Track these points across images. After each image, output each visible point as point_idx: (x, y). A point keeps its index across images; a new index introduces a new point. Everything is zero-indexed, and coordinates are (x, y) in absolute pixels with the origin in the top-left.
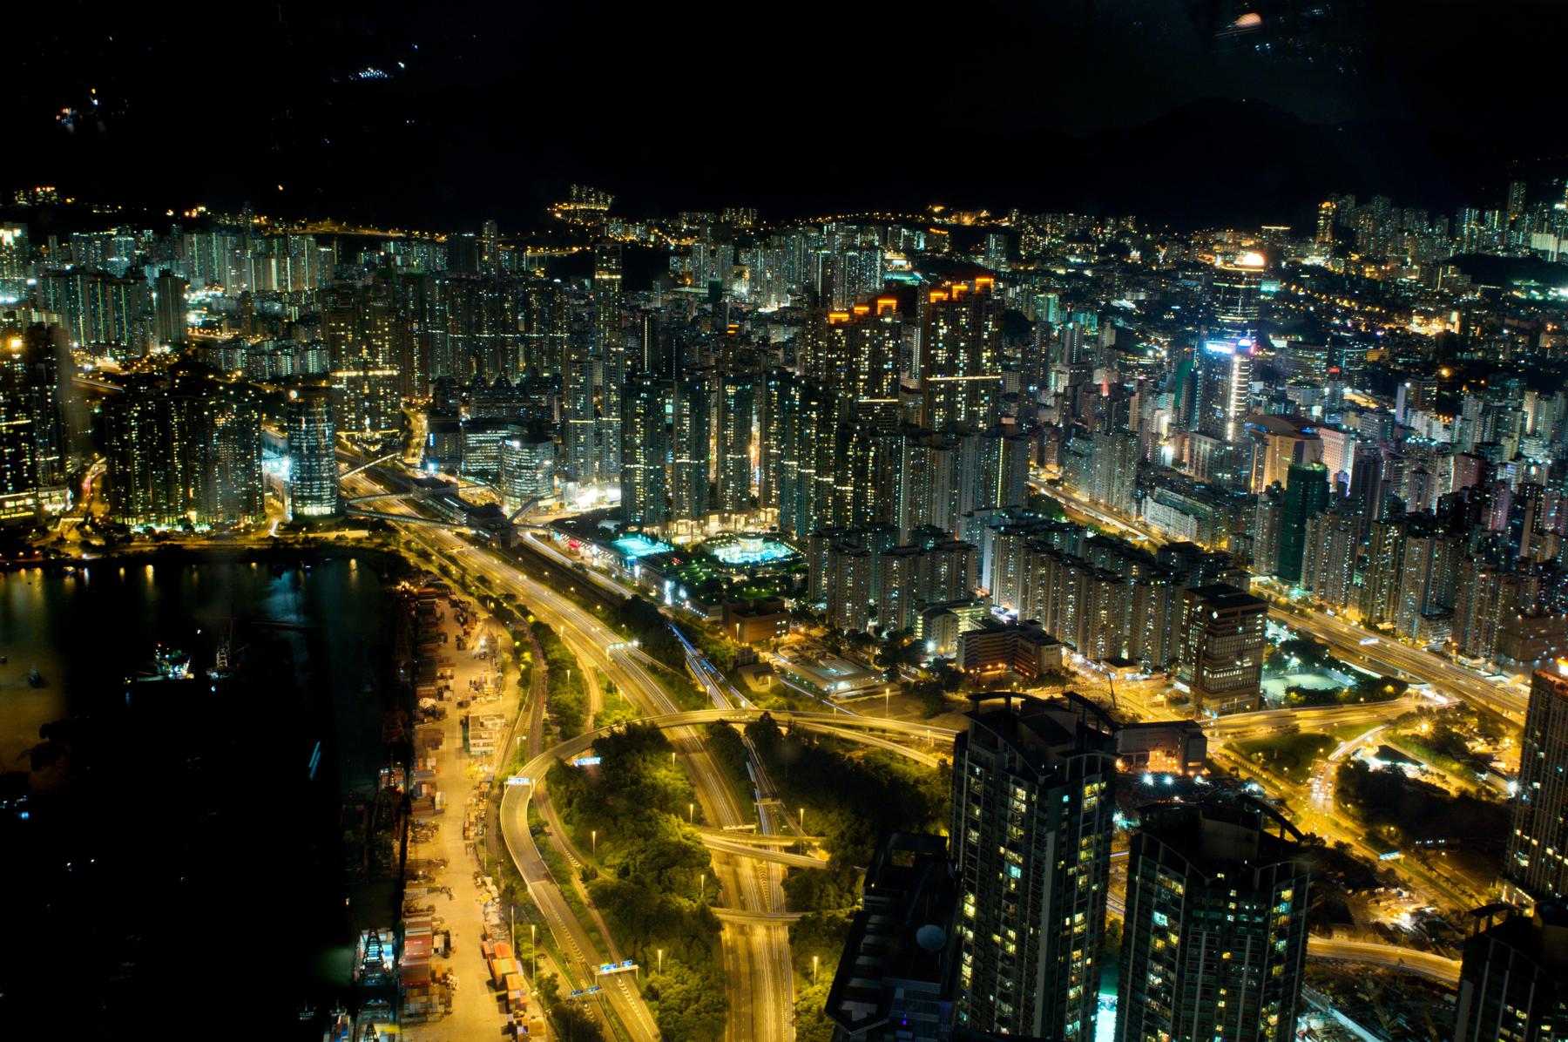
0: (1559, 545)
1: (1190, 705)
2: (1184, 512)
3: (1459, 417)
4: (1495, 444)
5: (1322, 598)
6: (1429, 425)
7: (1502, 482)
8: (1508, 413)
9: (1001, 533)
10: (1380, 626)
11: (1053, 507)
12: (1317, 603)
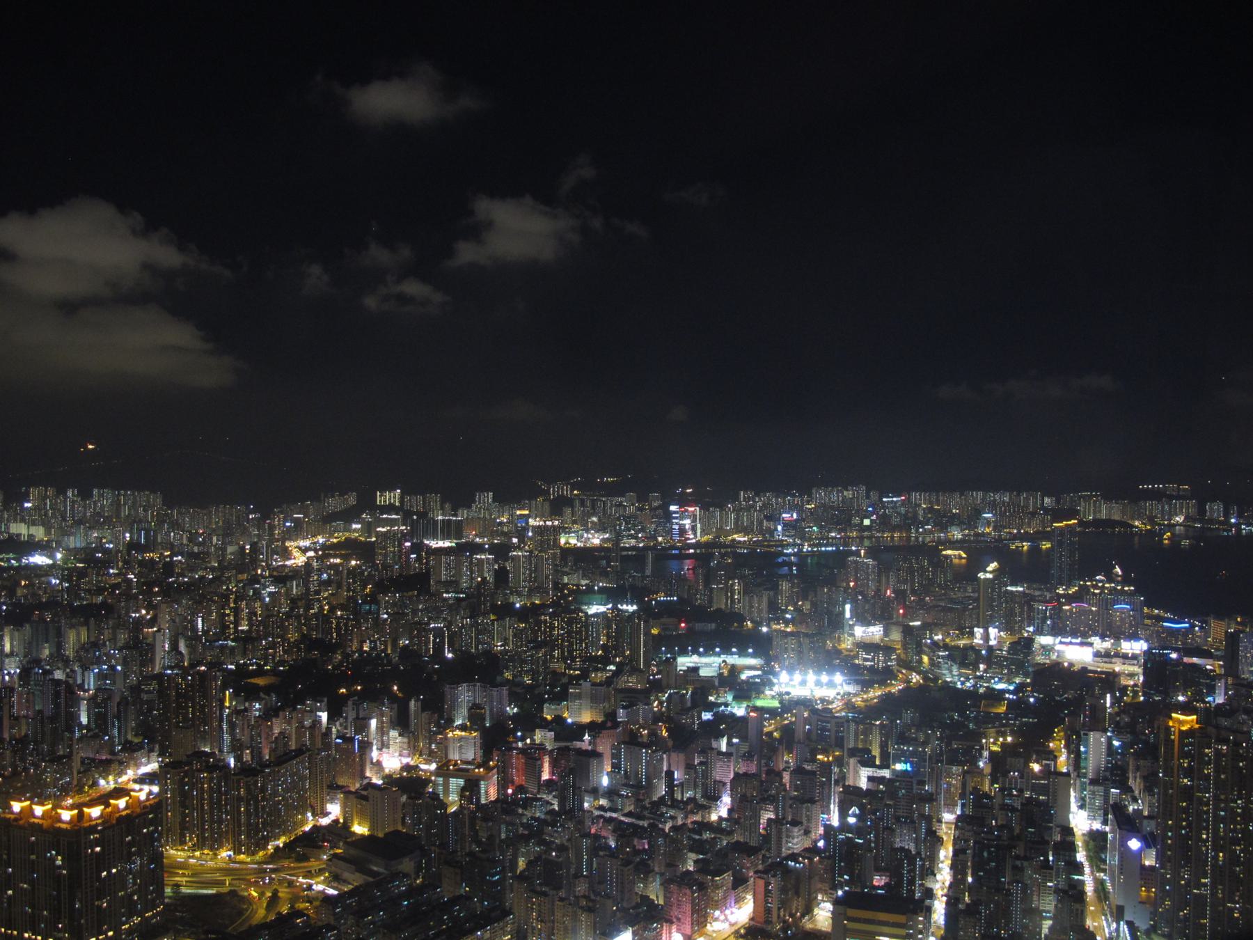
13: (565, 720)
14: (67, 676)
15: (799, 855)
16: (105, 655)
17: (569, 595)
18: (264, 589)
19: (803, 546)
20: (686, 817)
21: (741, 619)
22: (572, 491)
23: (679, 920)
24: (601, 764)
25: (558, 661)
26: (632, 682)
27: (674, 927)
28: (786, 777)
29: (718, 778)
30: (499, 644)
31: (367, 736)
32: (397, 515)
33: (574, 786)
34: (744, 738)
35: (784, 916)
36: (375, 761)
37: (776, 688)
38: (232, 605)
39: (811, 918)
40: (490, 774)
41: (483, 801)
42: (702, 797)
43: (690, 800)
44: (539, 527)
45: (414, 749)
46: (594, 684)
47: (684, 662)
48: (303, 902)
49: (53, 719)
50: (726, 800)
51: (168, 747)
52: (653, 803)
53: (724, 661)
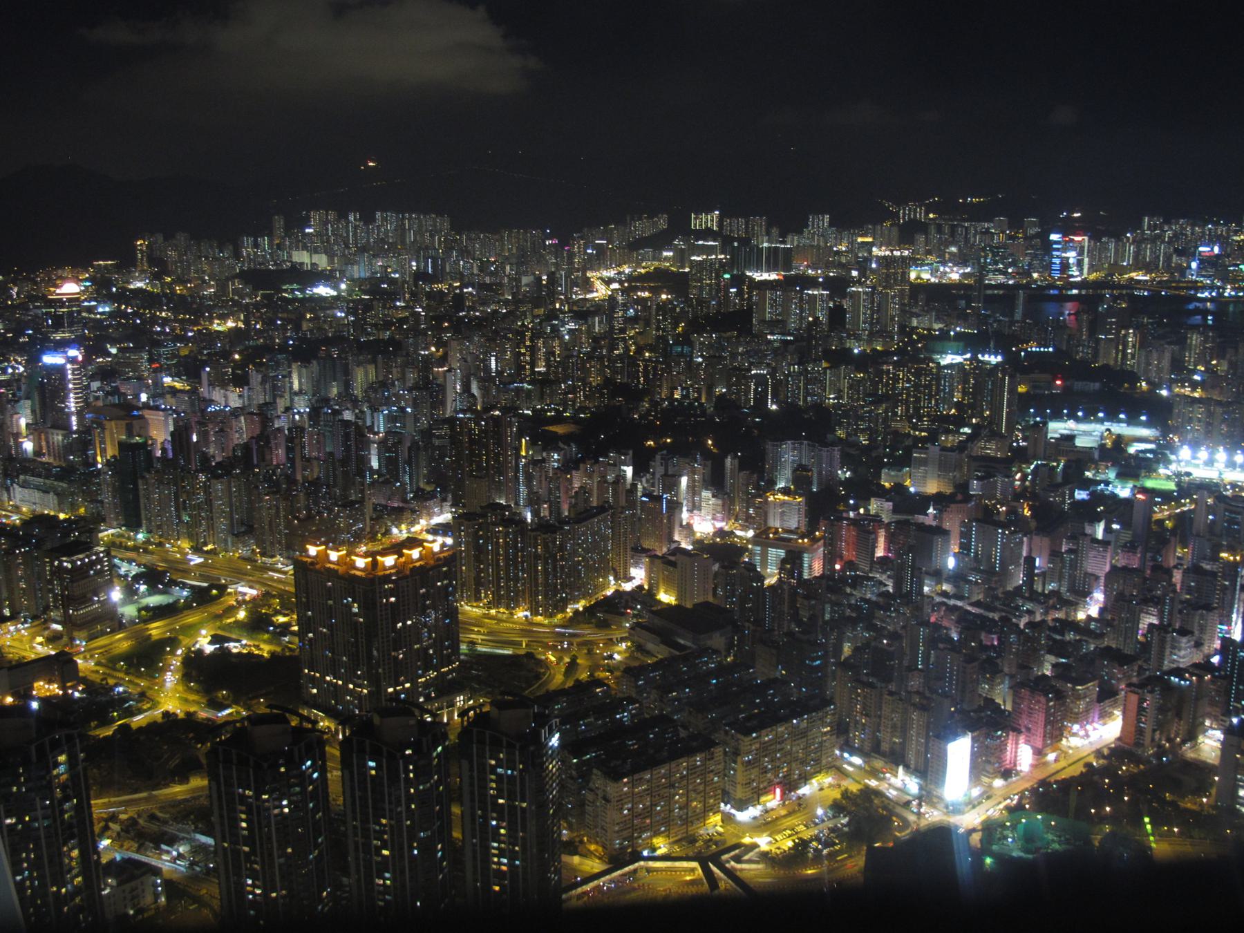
0: (320, 466)
1: (65, 639)
3: (246, 388)
4: (271, 405)
5: (161, 536)
6: (226, 397)
7: (278, 429)
8: (279, 380)
10: (205, 549)
12: (157, 541)
13: (907, 488)
14: (357, 417)
15: (1186, 670)
16: (394, 395)
17: (918, 341)
18: (563, 326)
19: (1224, 289)
20: (1046, 613)
21: (1133, 378)
22: (927, 214)
23: (1028, 729)
24: (947, 542)
25: (901, 419)
26: (990, 449)
27: (1022, 739)
28: (1177, 577)
29: (1090, 570)
30: (832, 396)
31: (676, 495)
32: (714, 241)
33: (913, 567)
34: (1126, 525)
35: (1160, 739)
36: (684, 523)
37: (1173, 467)
38: (528, 343)
39: (1194, 747)
40: (816, 546)
41: (806, 576)
42: (1068, 591)
43: (1054, 593)
44: (885, 257)
45: (728, 513)
46: (944, 449)
47: (1057, 428)
48: (604, 670)
49: (345, 462)
50: (1099, 596)
51: (462, 497)
52: (1007, 593)
53: (1108, 430)
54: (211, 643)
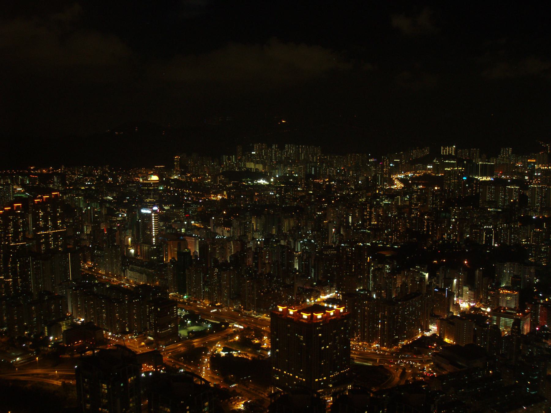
2: (141, 273)
4: (245, 235)
6: (222, 231)
9: (74, 290)
10: (217, 305)
11: (92, 277)
12: (193, 300)
14: (288, 243)
18: (382, 202)
30: (523, 240)
31: (451, 288)
32: (454, 161)
38: (368, 210)
40: (526, 317)
45: (476, 298)
54: (223, 351)
